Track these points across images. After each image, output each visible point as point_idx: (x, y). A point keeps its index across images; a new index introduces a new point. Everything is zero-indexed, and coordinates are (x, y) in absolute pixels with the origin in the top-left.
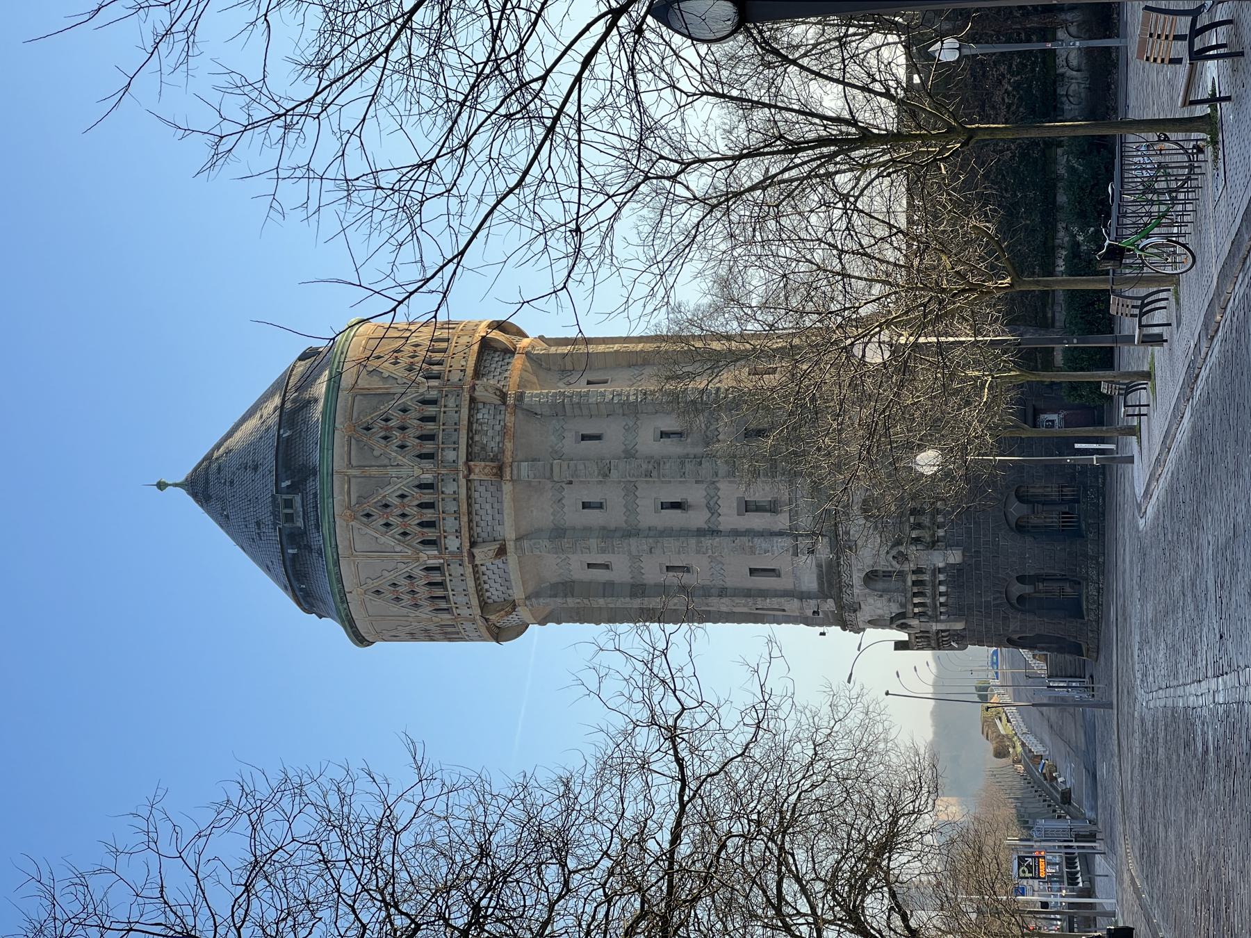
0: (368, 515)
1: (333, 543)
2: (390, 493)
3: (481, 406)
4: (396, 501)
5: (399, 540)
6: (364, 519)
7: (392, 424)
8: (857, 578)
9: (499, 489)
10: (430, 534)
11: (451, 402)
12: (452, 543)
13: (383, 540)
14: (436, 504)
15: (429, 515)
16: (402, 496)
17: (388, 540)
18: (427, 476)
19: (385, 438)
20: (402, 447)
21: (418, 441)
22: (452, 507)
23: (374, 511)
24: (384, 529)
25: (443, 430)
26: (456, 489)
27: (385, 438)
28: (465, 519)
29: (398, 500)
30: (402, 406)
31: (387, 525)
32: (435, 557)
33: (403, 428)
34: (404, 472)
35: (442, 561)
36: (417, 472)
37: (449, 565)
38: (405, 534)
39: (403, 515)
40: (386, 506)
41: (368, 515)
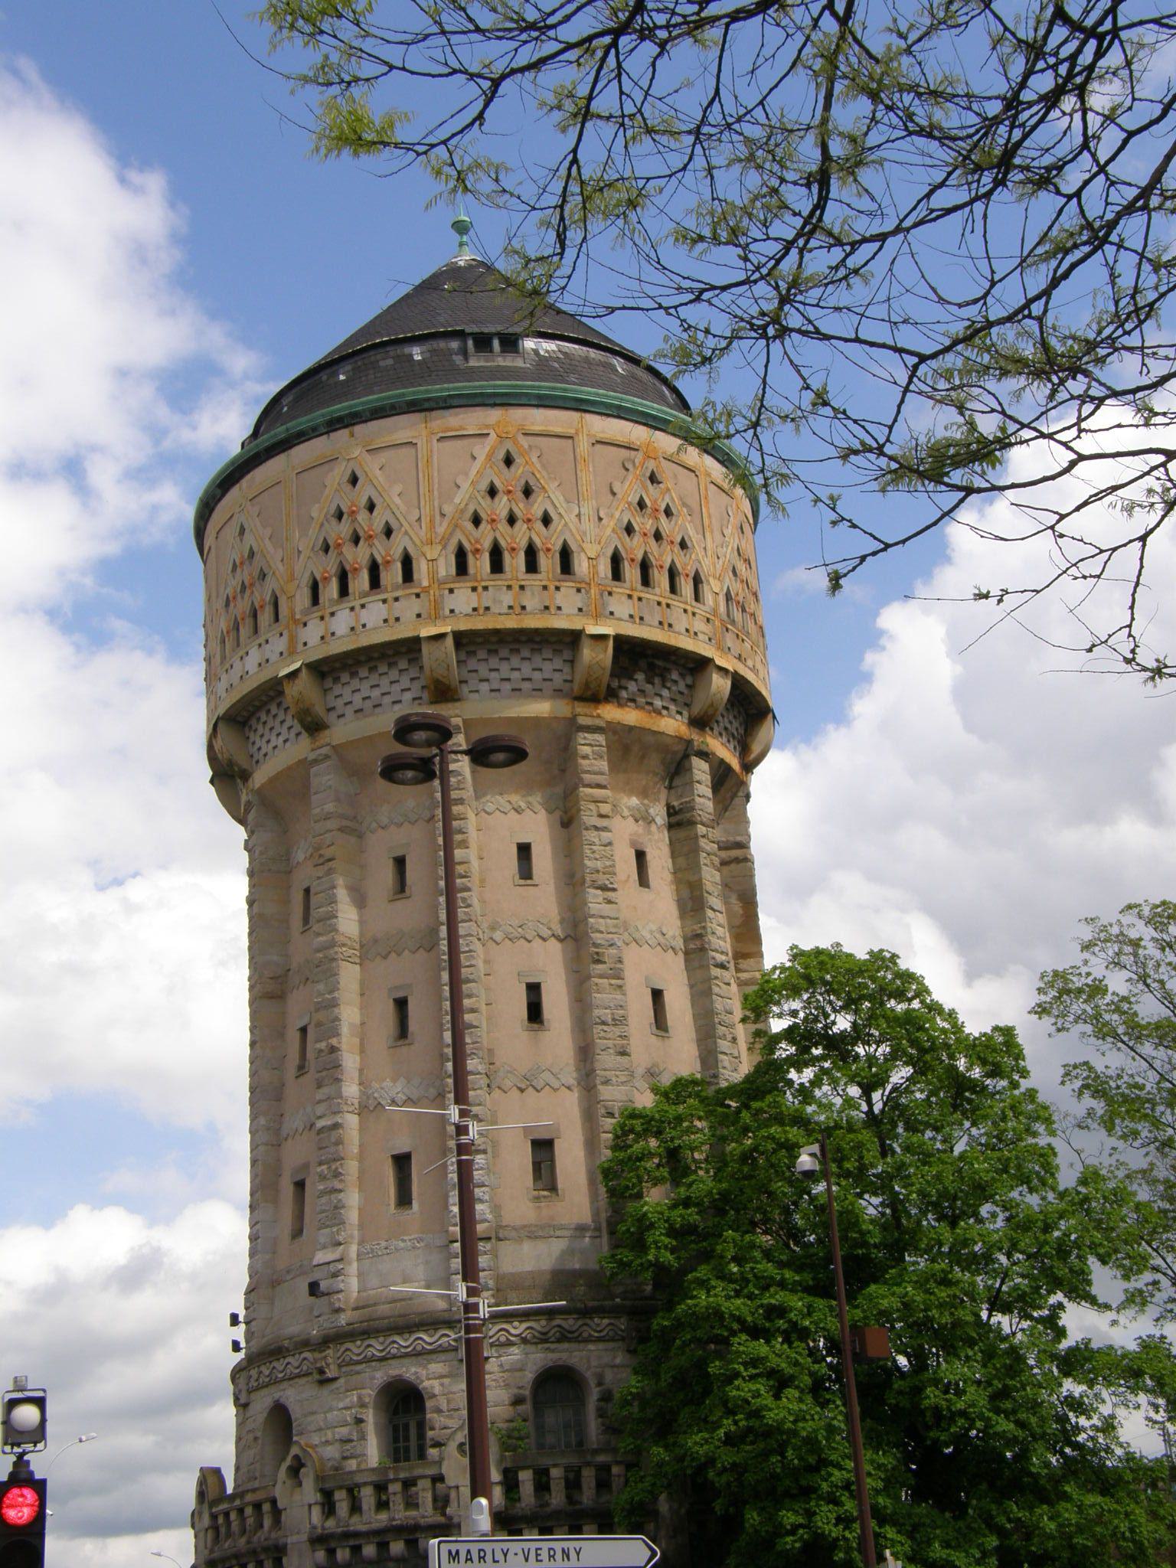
0: (509, 461)
1: (455, 402)
2: (552, 497)
3: (689, 681)
4: (537, 510)
5: (462, 511)
6: (501, 455)
7: (663, 518)
8: (410, 1371)
9: (558, 693)
10: (480, 565)
11: (699, 625)
12: (463, 600)
13: (465, 485)
14: (538, 576)
15: (515, 563)
16: (546, 520)
17: (466, 495)
18: (585, 564)
19: (641, 504)
20: (629, 530)
21: (640, 557)
22: (532, 601)
23: (519, 470)
24: (484, 485)
25: (659, 604)
26: (565, 610)
27: (641, 504)
28: (511, 623)
29: (540, 514)
30: (689, 544)
31: (492, 492)
32: (433, 575)
33: (658, 536)
34: (589, 526)
35: (425, 583)
36: (592, 550)
37: (418, 596)
38: (476, 521)
39: (512, 520)
40: (527, 492)
41: (509, 461)
